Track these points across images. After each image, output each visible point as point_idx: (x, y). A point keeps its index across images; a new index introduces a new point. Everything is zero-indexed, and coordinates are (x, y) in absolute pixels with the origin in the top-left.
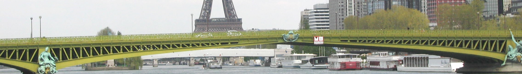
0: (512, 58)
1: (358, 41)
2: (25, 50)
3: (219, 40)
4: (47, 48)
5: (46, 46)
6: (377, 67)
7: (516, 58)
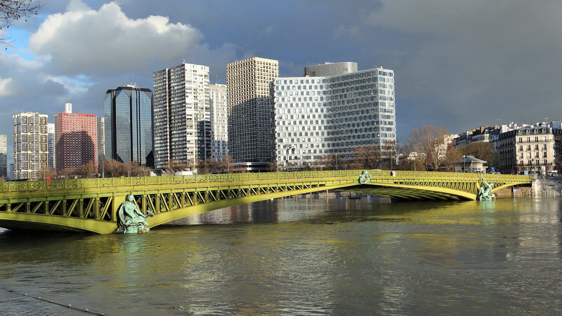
2: (94, 199)
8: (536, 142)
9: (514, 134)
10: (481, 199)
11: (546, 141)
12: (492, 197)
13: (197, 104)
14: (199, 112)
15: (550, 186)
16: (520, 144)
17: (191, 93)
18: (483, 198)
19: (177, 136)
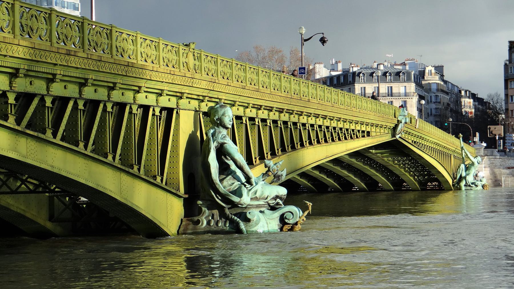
8: (389, 96)
9: (350, 79)
10: (463, 188)
11: (406, 95)
12: (483, 183)
15: (509, 168)
16: (388, 98)
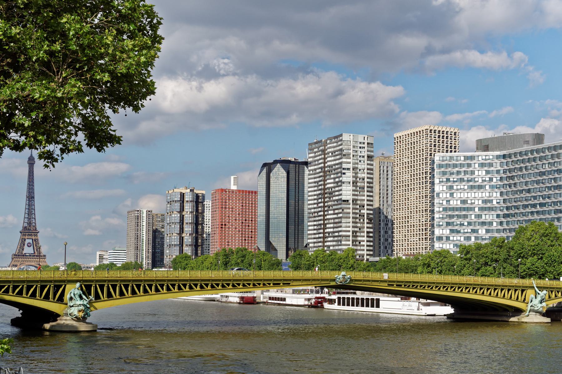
0: (538, 308)
1: (403, 286)
3: (271, 280)
4: (78, 284)
5: (76, 281)
6: (284, 302)
7: (541, 308)
13: (356, 183)
14: (358, 192)
17: (348, 169)
18: (531, 306)
19: (332, 221)
